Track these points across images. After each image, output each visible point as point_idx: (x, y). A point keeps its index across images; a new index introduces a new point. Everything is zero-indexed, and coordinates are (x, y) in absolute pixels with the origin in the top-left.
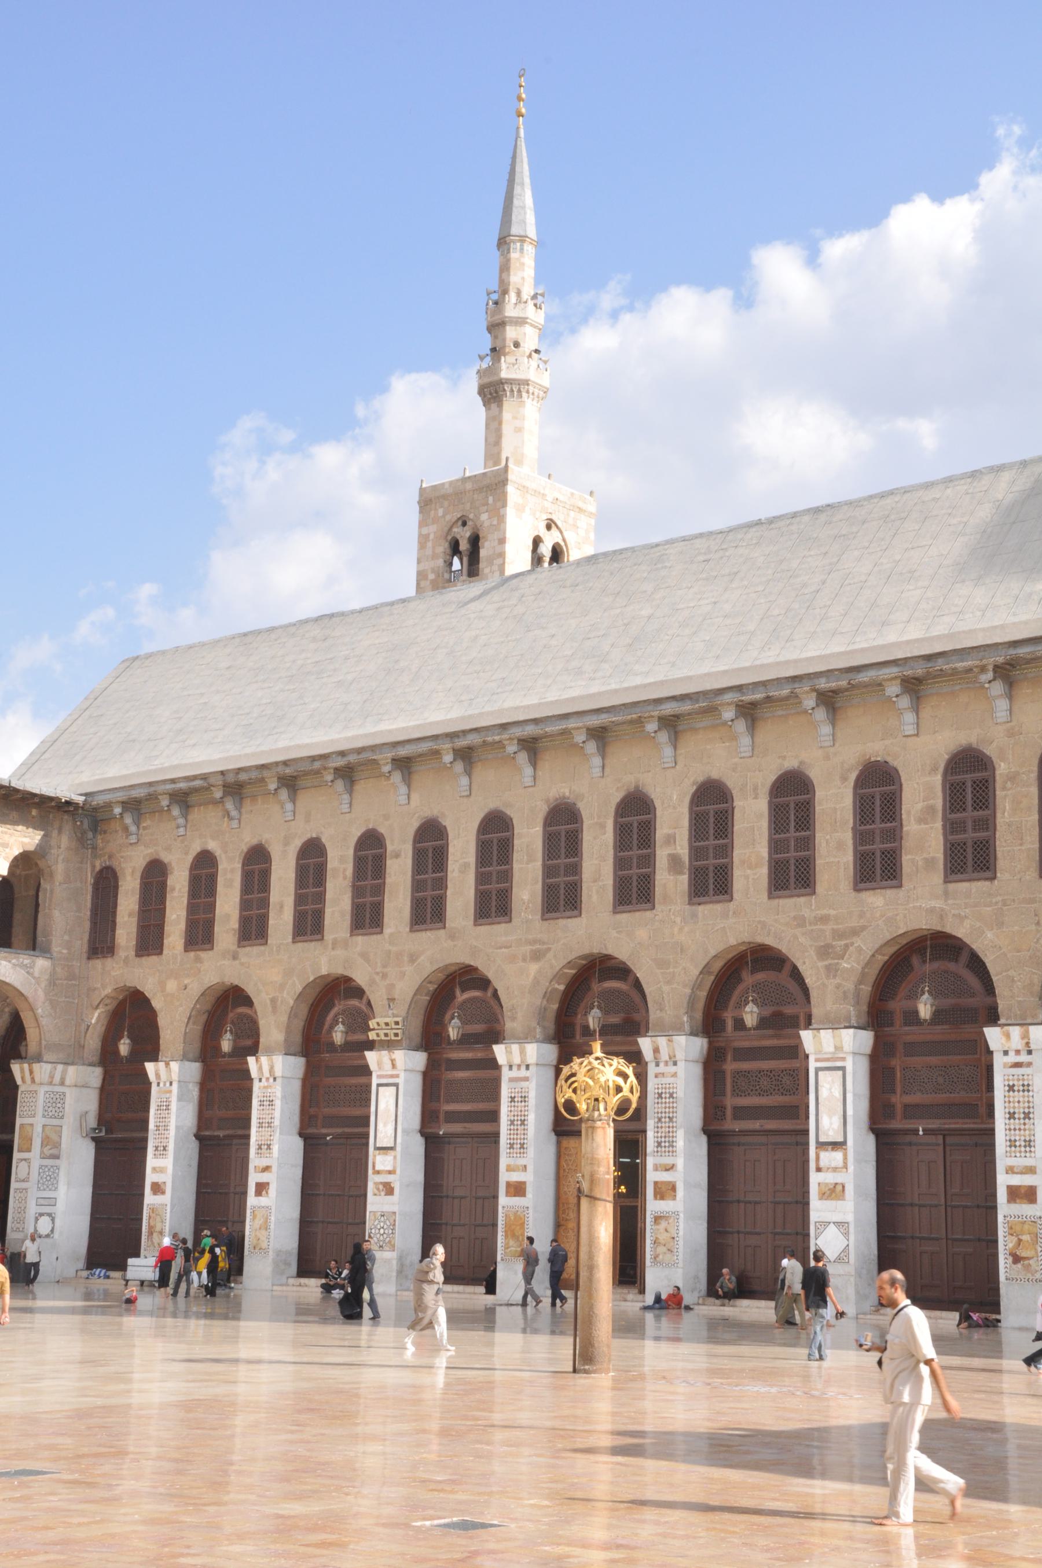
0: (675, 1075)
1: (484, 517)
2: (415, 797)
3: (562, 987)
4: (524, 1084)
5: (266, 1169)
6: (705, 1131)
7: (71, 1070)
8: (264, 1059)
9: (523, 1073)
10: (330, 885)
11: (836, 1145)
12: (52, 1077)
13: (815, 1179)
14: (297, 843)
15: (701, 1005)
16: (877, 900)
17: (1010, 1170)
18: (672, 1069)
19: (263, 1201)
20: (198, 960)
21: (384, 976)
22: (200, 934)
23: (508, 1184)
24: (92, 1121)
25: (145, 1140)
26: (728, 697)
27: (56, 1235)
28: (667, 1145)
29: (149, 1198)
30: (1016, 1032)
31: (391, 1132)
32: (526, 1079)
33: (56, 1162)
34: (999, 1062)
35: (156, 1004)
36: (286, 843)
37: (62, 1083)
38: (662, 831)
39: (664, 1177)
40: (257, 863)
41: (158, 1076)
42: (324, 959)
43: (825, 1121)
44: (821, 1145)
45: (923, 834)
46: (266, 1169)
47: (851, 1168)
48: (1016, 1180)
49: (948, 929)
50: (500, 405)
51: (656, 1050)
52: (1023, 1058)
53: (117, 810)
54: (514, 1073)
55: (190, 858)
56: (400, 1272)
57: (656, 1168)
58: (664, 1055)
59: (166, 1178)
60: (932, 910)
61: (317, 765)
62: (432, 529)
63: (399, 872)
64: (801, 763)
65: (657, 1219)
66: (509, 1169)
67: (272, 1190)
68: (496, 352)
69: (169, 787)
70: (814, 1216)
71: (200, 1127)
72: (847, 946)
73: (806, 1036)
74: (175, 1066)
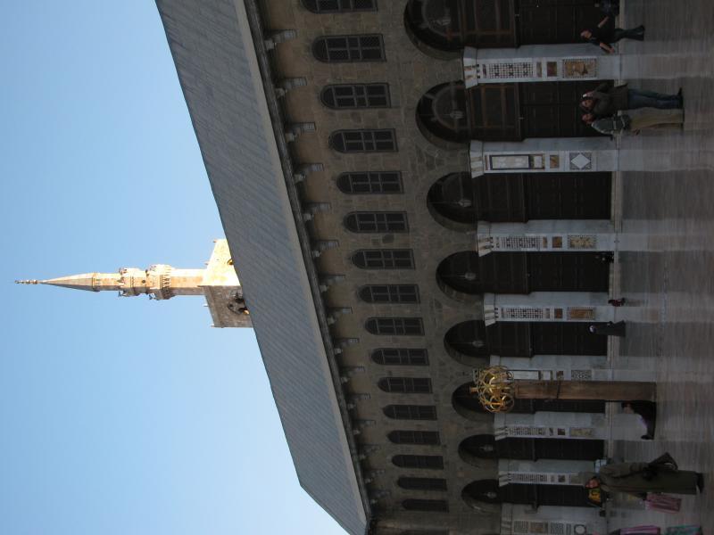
0: (498, 238)
1: (228, 296)
2: (360, 364)
3: (455, 292)
4: (505, 310)
5: (551, 430)
6: (526, 222)
7: (504, 519)
8: (497, 433)
9: (499, 311)
10: (406, 403)
11: (531, 159)
12: (507, 529)
13: (548, 170)
14: (386, 418)
15: (460, 225)
16: (402, 141)
17: (540, 75)
18: (495, 240)
19: (567, 431)
20: (447, 463)
21: (452, 377)
22: (435, 462)
23: (556, 317)
24: (529, 508)
25: (539, 486)
26: (299, 217)
27: (584, 524)
28: (533, 242)
29: (567, 483)
30: (467, 73)
31: (532, 373)
32: (502, 310)
33: (549, 525)
34: (483, 80)
35: (470, 481)
36: (386, 423)
37: (510, 523)
38: (371, 246)
39: (550, 242)
40: (395, 437)
41: (505, 481)
42: (445, 406)
43: (518, 165)
44: (531, 166)
45: (367, 118)
46: (551, 430)
47: (542, 152)
48: (545, 72)
49: (416, 105)
50: (173, 289)
51: (485, 248)
52: (481, 68)
53: (374, 502)
54: (500, 315)
55: (397, 468)
56: (601, 367)
57: (546, 247)
58: (488, 243)
59: (556, 476)
60: (405, 114)
61: (346, 413)
62: (235, 321)
63: (398, 371)
64: (332, 179)
65: (572, 246)
66: (548, 317)
67: (562, 427)
68: (148, 291)
69: (361, 480)
70: (568, 170)
71: (531, 459)
72: (427, 155)
73: (474, 175)
74: (500, 473)
